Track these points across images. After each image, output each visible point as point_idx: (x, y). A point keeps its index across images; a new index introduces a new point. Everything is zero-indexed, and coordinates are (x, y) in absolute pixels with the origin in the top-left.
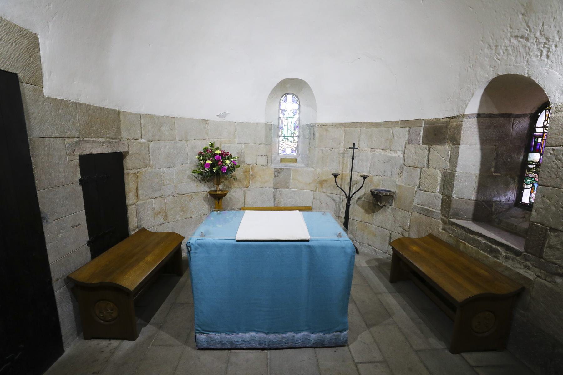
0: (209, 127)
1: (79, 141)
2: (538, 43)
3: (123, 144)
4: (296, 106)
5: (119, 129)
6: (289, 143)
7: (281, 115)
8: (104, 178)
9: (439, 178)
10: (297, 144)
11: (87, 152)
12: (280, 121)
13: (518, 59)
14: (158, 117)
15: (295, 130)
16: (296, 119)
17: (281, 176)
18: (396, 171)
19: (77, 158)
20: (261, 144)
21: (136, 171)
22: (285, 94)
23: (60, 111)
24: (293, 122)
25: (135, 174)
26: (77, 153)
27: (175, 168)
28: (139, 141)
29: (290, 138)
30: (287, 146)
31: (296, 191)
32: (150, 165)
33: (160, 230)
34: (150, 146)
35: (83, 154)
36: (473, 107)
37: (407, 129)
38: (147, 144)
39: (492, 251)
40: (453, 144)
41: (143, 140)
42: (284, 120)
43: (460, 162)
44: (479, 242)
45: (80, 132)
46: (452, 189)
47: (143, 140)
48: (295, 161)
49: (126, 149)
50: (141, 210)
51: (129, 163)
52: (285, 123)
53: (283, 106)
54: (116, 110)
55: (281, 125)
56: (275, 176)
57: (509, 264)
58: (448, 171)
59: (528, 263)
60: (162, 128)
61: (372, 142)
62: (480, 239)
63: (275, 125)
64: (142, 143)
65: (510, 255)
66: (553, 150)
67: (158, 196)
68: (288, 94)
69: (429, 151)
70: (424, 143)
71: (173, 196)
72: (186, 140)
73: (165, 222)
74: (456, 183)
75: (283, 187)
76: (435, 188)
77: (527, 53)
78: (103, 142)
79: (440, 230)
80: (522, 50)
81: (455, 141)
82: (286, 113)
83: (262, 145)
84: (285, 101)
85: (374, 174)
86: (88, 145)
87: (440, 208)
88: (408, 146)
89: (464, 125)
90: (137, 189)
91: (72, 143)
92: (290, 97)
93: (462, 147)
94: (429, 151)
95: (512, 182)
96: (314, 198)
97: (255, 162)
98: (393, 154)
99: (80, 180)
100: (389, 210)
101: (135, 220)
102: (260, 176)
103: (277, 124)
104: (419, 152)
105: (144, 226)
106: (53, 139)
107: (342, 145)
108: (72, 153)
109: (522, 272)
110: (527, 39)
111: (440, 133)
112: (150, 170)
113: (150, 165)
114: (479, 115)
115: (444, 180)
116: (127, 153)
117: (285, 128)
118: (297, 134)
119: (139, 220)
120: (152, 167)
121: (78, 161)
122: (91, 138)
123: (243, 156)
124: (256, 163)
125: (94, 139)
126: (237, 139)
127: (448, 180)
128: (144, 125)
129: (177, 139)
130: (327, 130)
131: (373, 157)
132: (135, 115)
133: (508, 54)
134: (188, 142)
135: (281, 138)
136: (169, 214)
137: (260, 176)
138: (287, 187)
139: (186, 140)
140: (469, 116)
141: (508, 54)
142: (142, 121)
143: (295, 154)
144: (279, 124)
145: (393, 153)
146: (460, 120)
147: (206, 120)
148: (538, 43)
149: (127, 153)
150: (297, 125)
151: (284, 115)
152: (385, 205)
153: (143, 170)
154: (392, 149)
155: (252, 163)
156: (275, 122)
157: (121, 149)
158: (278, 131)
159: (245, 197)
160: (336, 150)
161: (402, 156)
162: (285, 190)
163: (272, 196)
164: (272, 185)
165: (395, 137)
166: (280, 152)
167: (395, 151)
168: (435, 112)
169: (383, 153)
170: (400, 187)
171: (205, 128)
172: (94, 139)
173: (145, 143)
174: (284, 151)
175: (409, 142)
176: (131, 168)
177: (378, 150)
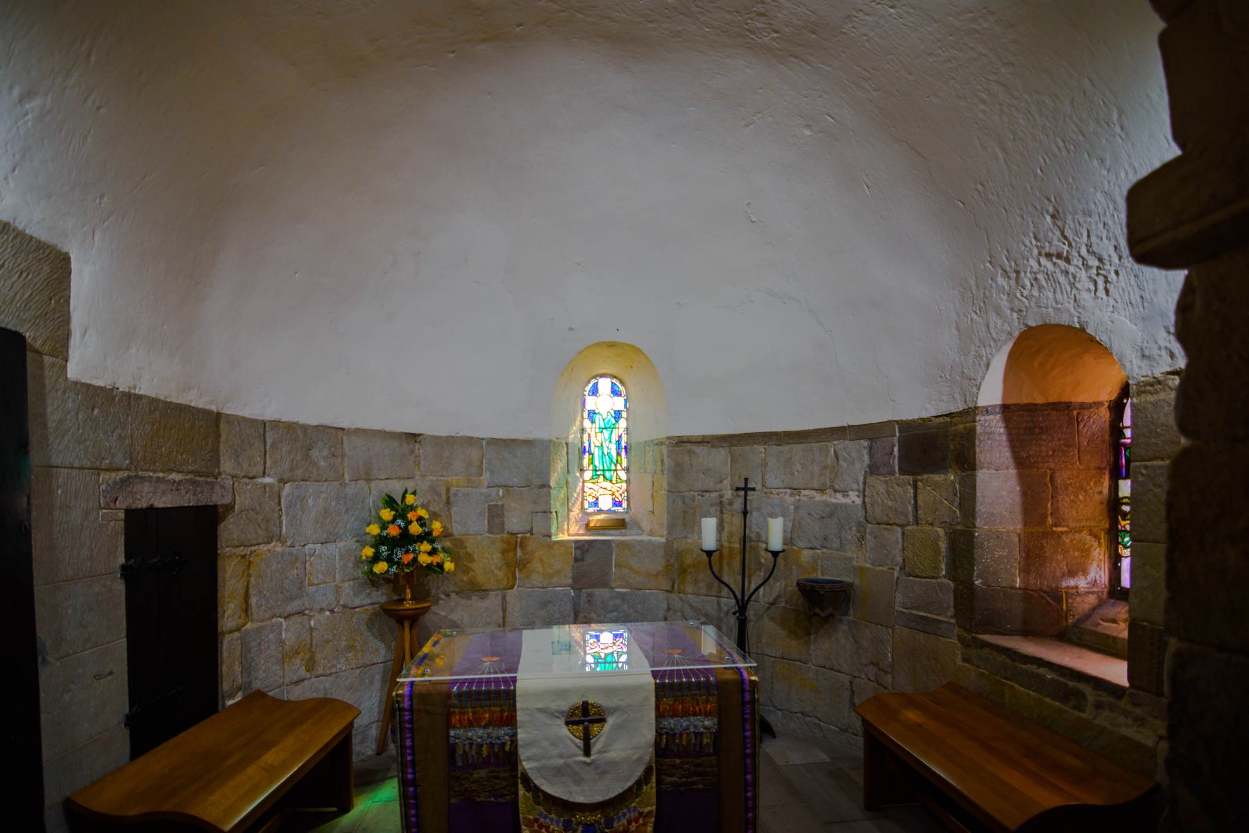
1: (129, 477)
2: (1087, 267)
3: (223, 487)
4: (619, 403)
5: (215, 453)
6: (607, 485)
7: (587, 423)
8: (175, 563)
9: (943, 546)
10: (624, 485)
11: (143, 504)
12: (586, 436)
13: (1059, 296)
15: (619, 454)
16: (621, 431)
17: (589, 559)
18: (851, 534)
19: (122, 515)
21: (247, 551)
22: (595, 377)
23: (96, 411)
24: (615, 438)
25: (244, 557)
26: (122, 504)
27: (340, 544)
28: (260, 480)
29: (607, 474)
30: (601, 491)
31: (625, 594)
32: (281, 539)
33: (297, 694)
35: (134, 507)
36: (991, 392)
37: (865, 443)
38: (276, 489)
39: (1066, 695)
40: (963, 469)
41: (268, 480)
42: (593, 435)
43: (980, 508)
44: (1041, 678)
45: (131, 459)
46: (972, 565)
47: (268, 480)
49: (227, 500)
50: (254, 644)
51: (229, 531)
52: (596, 441)
53: (591, 403)
55: (586, 445)
56: (576, 560)
57: (1103, 719)
58: (958, 527)
59: (1138, 711)
61: (792, 474)
62: (1042, 671)
64: (265, 486)
65: (1106, 698)
66: (1146, 467)
67: (295, 610)
68: (602, 376)
69: (915, 487)
70: (903, 471)
72: (368, 480)
74: (977, 552)
75: (594, 586)
76: (937, 568)
77: (1072, 285)
78: (180, 481)
79: (960, 662)
80: (1062, 279)
81: (966, 462)
82: (597, 418)
84: (595, 391)
85: (801, 544)
86: (146, 487)
87: (951, 612)
88: (870, 480)
89: (979, 429)
90: (247, 595)
91: (115, 483)
93: (982, 475)
94: (915, 487)
95: (1096, 544)
97: (528, 528)
98: (840, 499)
99: (124, 568)
100: (844, 627)
101: (238, 668)
102: (541, 561)
104: (895, 491)
105: (257, 685)
106: (75, 472)
107: (727, 482)
108: (112, 505)
109: (1131, 732)
110: (1068, 260)
111: (935, 447)
112: (279, 549)
113: (281, 539)
114: (1005, 408)
115: (952, 547)
116: (230, 508)
117: (596, 451)
118: (625, 464)
119: (247, 669)
120: (283, 543)
121: (122, 523)
122: (155, 471)
123: (502, 515)
124: (531, 532)
125: (161, 475)
126: (486, 477)
127: (962, 546)
129: (347, 477)
130: (690, 452)
131: (797, 508)
133: (1040, 288)
134: (373, 484)
135: (588, 475)
137: (541, 561)
138: (605, 585)
139: (368, 480)
140: (987, 410)
141: (1040, 288)
144: (582, 443)
145: (839, 495)
146: (970, 418)
147: (414, 436)
148: (1087, 267)
149: (230, 508)
150: (623, 444)
151: (593, 422)
152: (831, 615)
153: (264, 548)
154: (837, 487)
157: (218, 498)
158: (581, 459)
159: (504, 610)
160: (714, 495)
161: (859, 501)
162: (598, 592)
163: (569, 607)
164: (570, 581)
165: (841, 462)
166: (586, 505)
167: (845, 493)
168: (918, 404)
169: (818, 497)
170: (861, 570)
171: (412, 452)
172: (161, 475)
173: (271, 486)
174: (596, 504)
175: (873, 470)
176: (236, 543)
177: (806, 492)
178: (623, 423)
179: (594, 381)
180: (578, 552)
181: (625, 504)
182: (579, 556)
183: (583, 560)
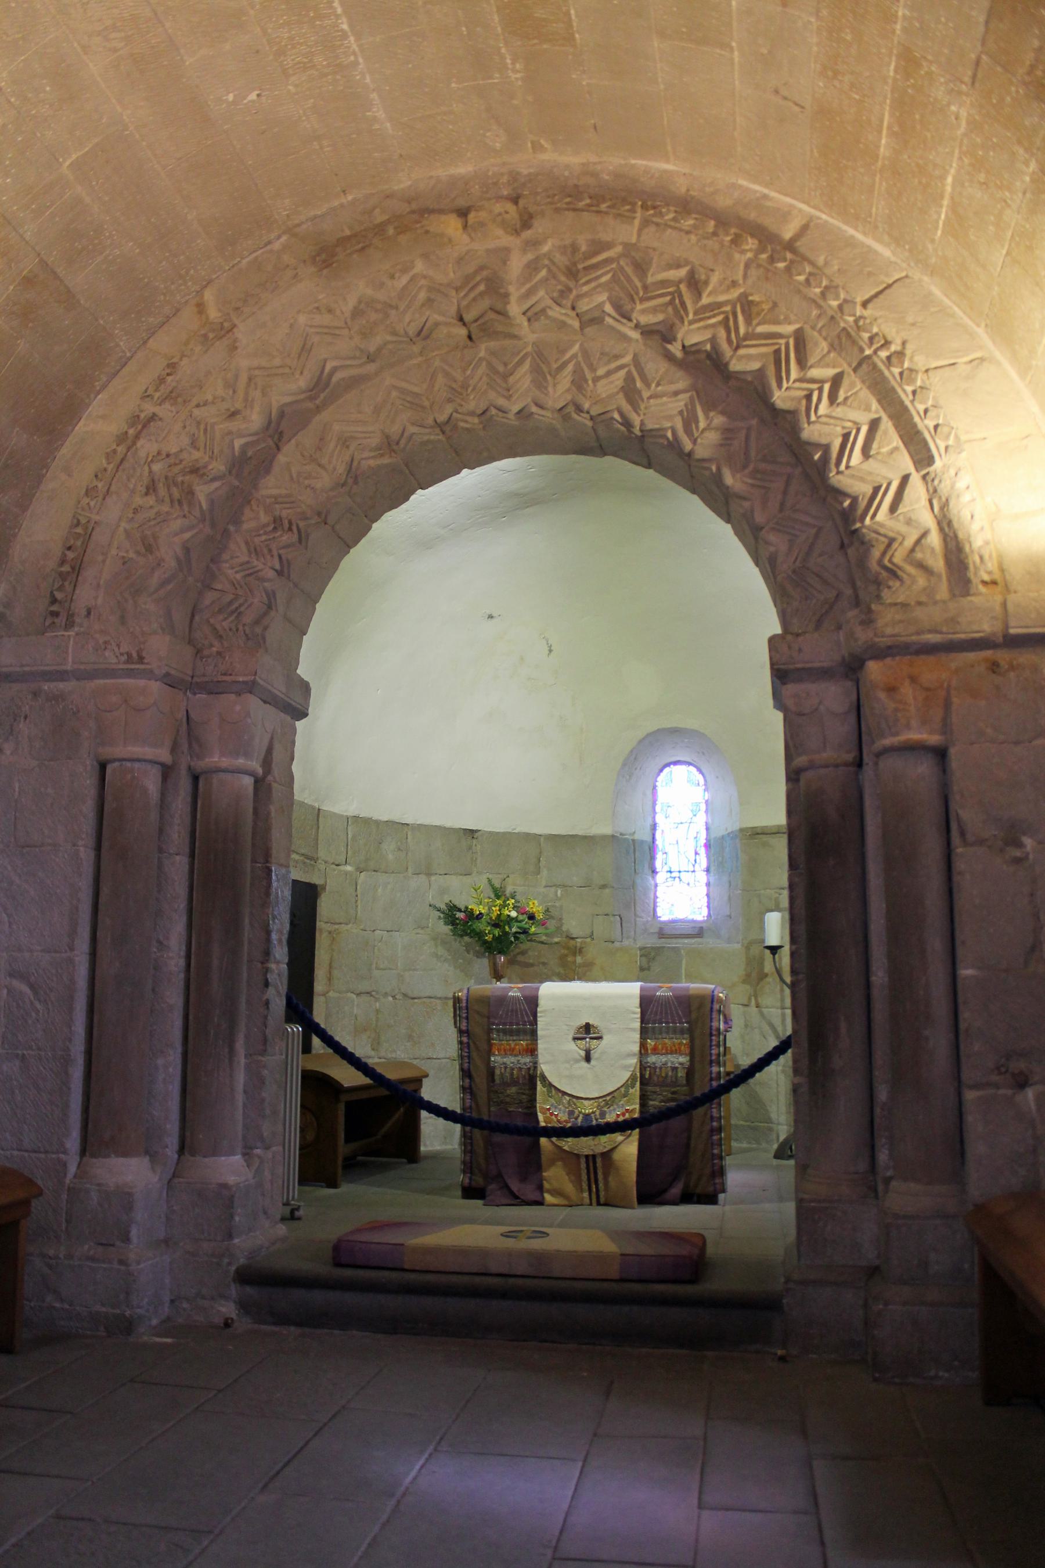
0: (479, 847)
7: (659, 819)
14: (378, 823)
15: (696, 853)
20: (604, 887)
25: (330, 933)
28: (342, 868)
34: (360, 882)
41: (349, 868)
47: (349, 868)
48: (698, 931)
54: (313, 808)
60: (384, 846)
63: (642, 842)
64: (346, 873)
68: (675, 763)
71: (394, 997)
72: (429, 874)
73: (373, 1053)
83: (607, 891)
92: (680, 772)
96: (746, 1026)
97: (588, 932)
103: (647, 838)
116: (324, 887)
117: (671, 850)
118: (704, 865)
124: (591, 936)
128: (354, 837)
129: (410, 870)
132: (339, 816)
134: (433, 878)
135: (660, 878)
136: (383, 1038)
139: (429, 874)
142: (350, 828)
143: (700, 918)
147: (471, 833)
150: (703, 841)
153: (344, 927)
155: (581, 934)
156: (644, 835)
157: (315, 879)
171: (470, 848)
178: (702, 818)
179: (667, 770)
180: (644, 959)
181: (705, 912)
182: (645, 965)
183: (649, 969)
